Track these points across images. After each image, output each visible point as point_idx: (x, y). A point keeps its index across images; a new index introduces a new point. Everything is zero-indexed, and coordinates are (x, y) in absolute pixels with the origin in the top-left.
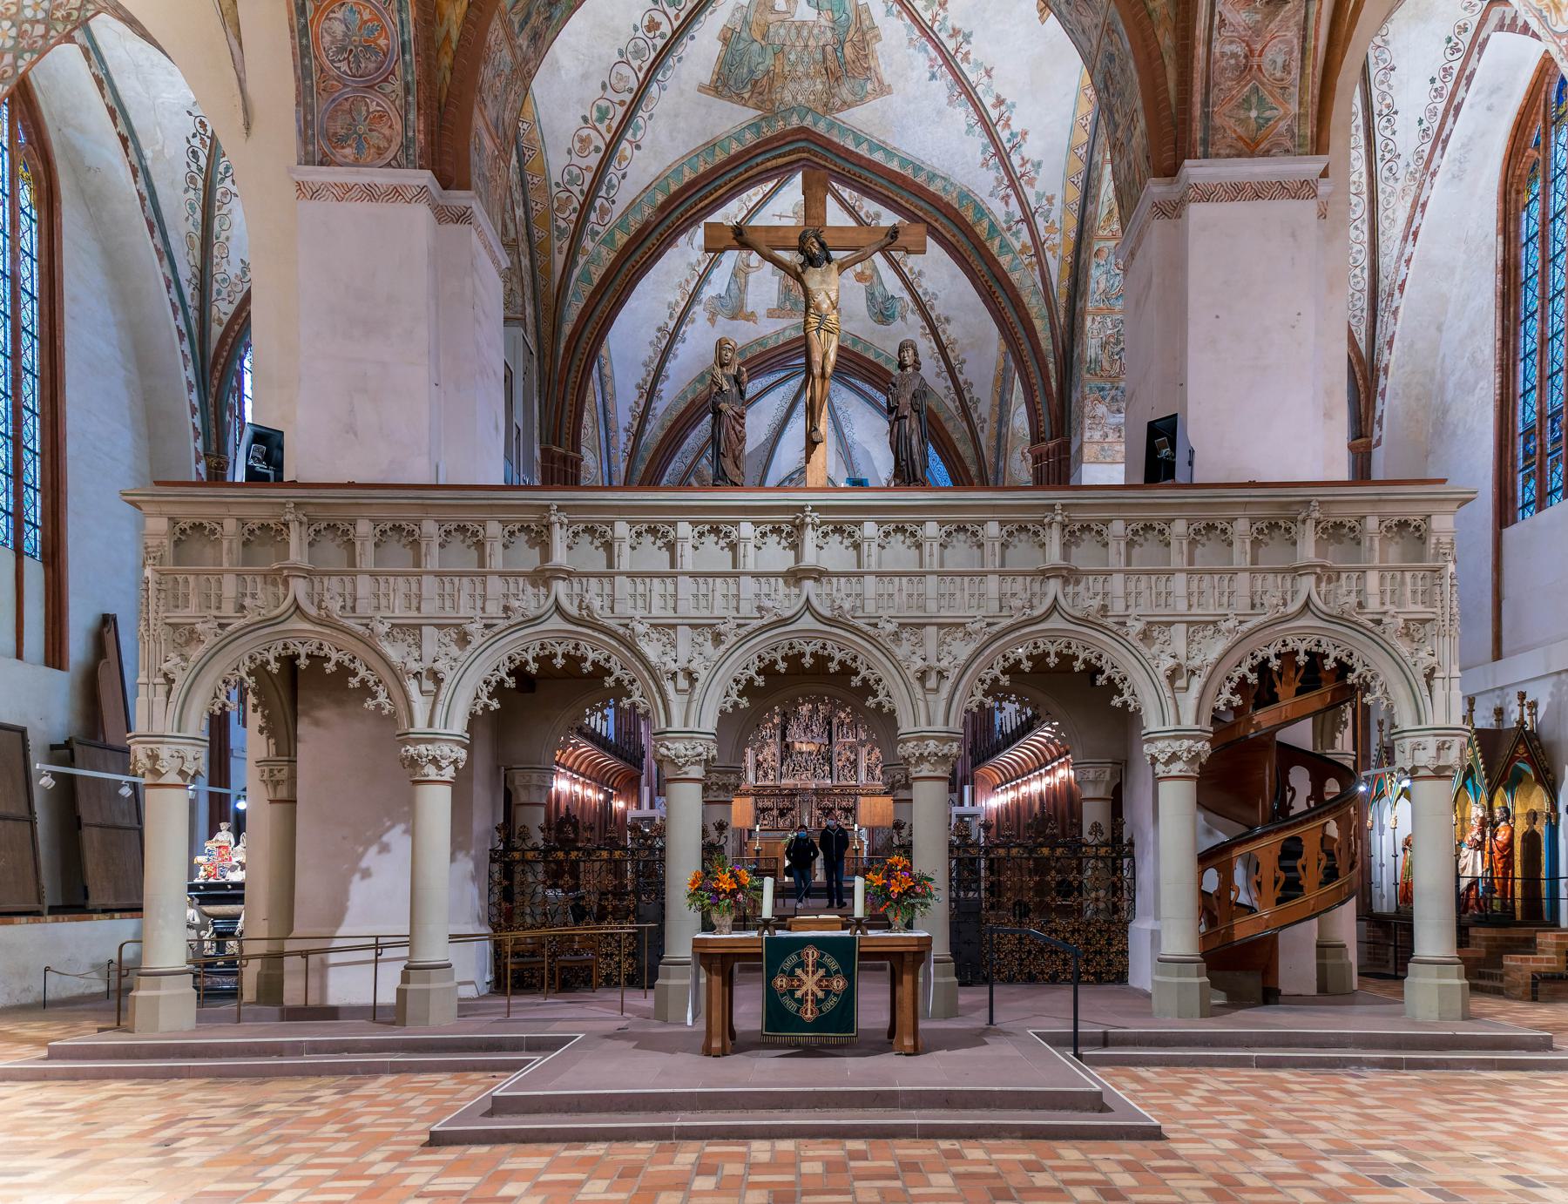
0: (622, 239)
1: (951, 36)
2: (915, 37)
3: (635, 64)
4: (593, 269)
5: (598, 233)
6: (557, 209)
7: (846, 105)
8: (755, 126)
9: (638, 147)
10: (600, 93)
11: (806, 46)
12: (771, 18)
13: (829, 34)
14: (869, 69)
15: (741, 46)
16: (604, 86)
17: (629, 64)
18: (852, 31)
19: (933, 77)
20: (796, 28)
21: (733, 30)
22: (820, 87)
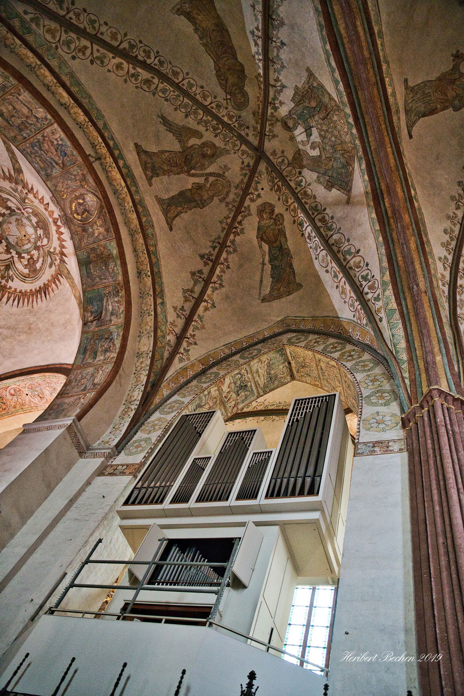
0: (387, 278)
1: (258, 46)
2: (279, 66)
3: (319, 250)
4: (390, 307)
5: (379, 295)
6: (361, 321)
7: (331, 98)
8: (360, 159)
9: (358, 251)
10: (329, 274)
11: (327, 131)
12: (324, 157)
13: (316, 118)
14: (309, 87)
15: (335, 175)
16: (327, 271)
17: (318, 254)
18: (307, 104)
19: (283, 44)
20: (323, 139)
21: (328, 181)
22: (335, 118)
